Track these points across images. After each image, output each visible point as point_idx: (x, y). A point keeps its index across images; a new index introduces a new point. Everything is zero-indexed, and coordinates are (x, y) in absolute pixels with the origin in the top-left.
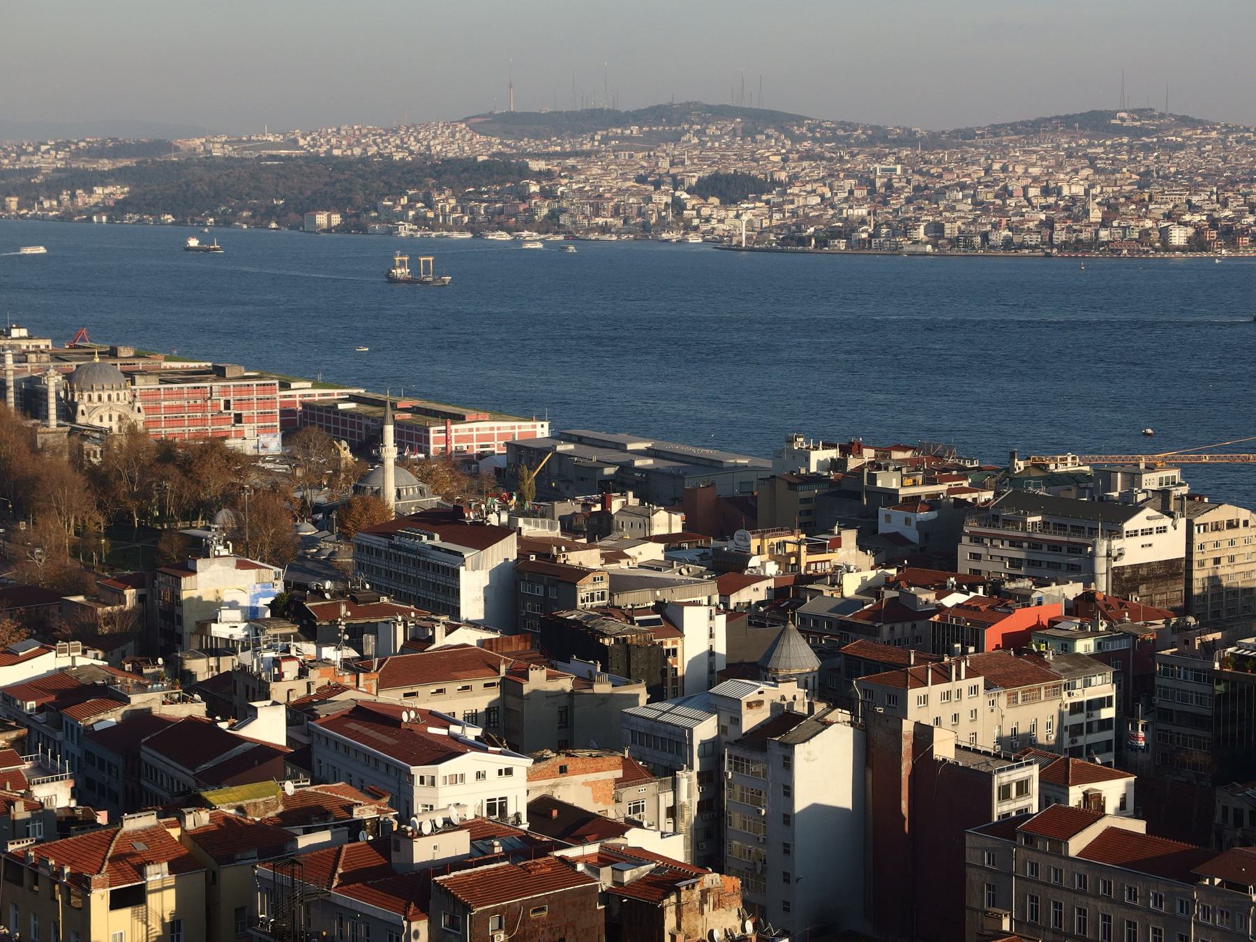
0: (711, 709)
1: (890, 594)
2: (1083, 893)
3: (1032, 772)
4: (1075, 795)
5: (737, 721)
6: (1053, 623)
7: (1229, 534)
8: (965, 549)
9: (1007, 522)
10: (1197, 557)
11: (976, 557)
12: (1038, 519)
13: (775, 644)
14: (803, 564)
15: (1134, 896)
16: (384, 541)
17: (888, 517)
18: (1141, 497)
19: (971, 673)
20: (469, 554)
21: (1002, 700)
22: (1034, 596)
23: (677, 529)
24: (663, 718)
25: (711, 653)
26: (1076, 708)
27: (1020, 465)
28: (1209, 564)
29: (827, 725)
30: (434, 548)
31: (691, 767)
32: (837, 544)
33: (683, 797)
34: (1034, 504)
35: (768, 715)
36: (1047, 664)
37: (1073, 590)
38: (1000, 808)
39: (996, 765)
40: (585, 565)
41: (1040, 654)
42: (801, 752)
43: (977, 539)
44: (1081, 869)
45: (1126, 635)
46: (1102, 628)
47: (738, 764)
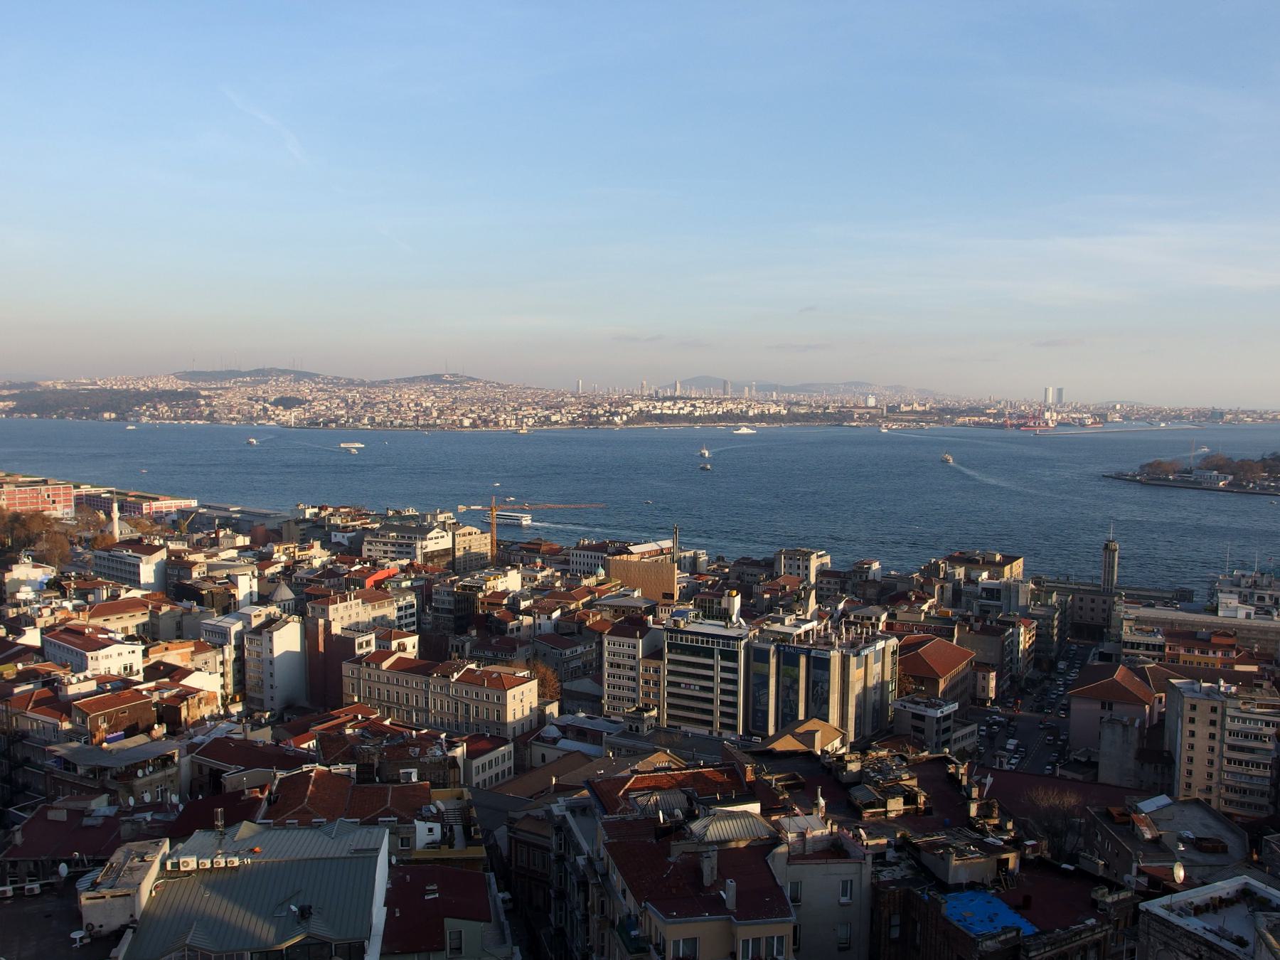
0: (239, 619)
1: (330, 567)
2: (389, 683)
3: (372, 637)
4: (394, 644)
5: (250, 623)
6: (394, 575)
7: (470, 537)
8: (365, 547)
9: (382, 536)
10: (457, 547)
11: (370, 550)
12: (394, 534)
13: (276, 589)
14: (297, 555)
15: (407, 683)
16: (107, 553)
17: (336, 535)
18: (435, 524)
19: (356, 598)
20: (144, 558)
21: (369, 608)
22: (387, 565)
23: (248, 543)
24: (220, 624)
25: (251, 594)
26: (400, 609)
27: (391, 513)
28: (462, 549)
29: (287, 623)
30: (129, 556)
31: (230, 644)
32: (312, 547)
33: (227, 656)
34: (393, 528)
35: (264, 619)
36: (388, 592)
37: (405, 562)
38: (359, 652)
39: (356, 634)
40: (197, 560)
41: (386, 587)
42: (276, 634)
43: (370, 543)
44: (388, 674)
45: (422, 579)
46: (413, 577)
47: (251, 641)
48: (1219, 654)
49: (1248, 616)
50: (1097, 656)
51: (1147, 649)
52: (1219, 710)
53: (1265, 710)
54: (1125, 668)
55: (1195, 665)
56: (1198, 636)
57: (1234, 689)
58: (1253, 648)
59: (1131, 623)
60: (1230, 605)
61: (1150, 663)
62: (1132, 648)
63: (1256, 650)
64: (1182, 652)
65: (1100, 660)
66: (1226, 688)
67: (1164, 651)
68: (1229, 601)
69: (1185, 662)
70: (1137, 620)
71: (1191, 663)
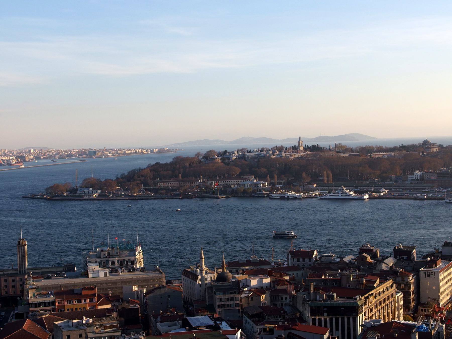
48: (88, 301)
49: (105, 274)
50: (14, 316)
51: (45, 306)
52: (84, 336)
53: (108, 330)
54: (30, 321)
55: (74, 310)
56: (75, 292)
57: (91, 321)
58: (109, 294)
59: (34, 291)
60: (94, 270)
61: (46, 314)
62: (36, 307)
63: (110, 295)
64: (66, 303)
65: (16, 319)
66: (86, 321)
67: (55, 305)
68: (94, 267)
69: (68, 310)
70: (37, 288)
71: (72, 309)
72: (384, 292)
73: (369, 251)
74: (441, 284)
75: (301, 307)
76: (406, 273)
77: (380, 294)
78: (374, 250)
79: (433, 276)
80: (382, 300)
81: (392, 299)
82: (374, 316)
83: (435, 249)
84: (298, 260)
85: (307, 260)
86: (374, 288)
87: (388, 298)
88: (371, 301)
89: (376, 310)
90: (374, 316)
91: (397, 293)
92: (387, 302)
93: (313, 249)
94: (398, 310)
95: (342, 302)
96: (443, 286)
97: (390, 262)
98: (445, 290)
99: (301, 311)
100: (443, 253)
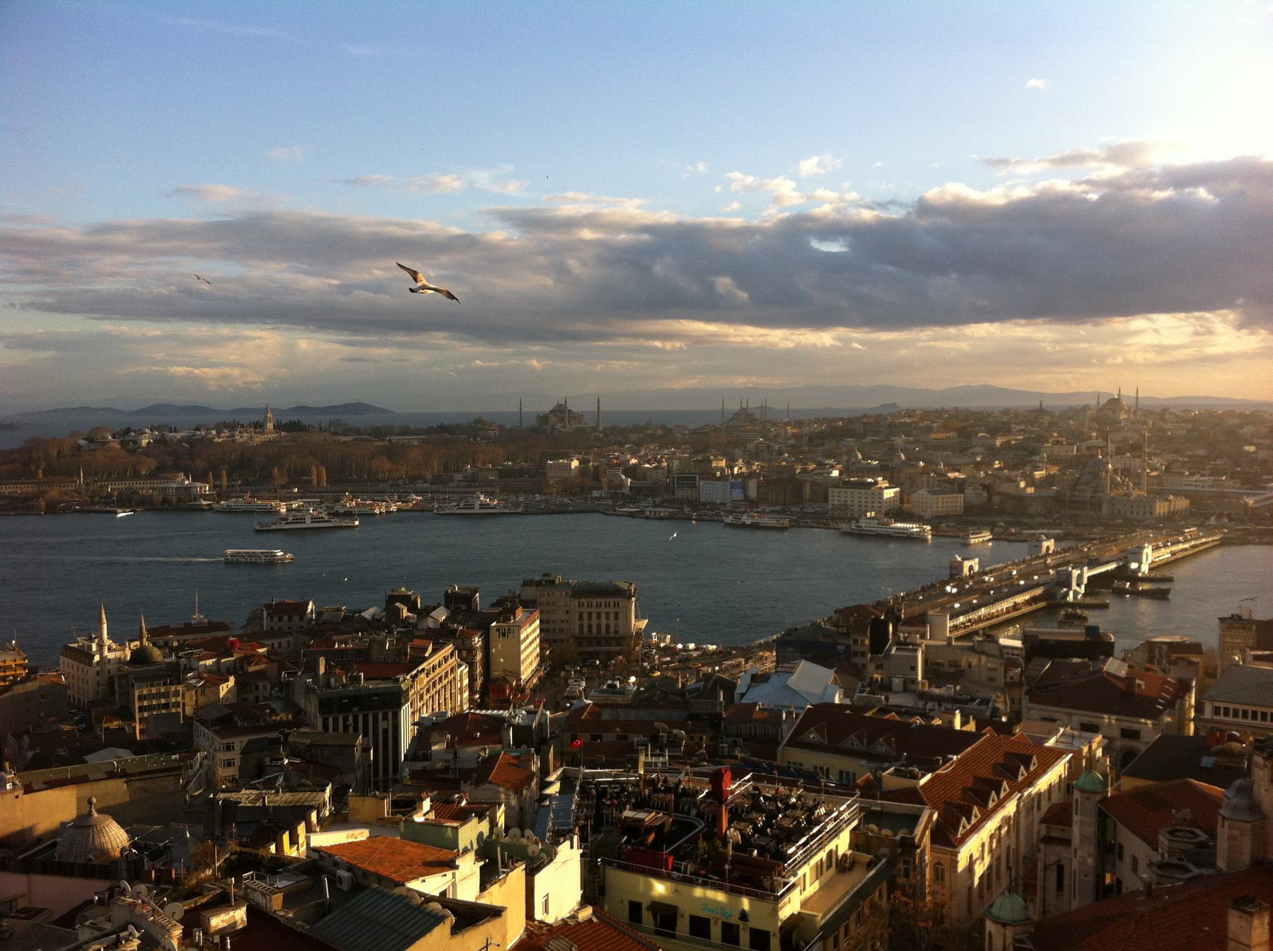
72: (440, 665)
73: (405, 599)
74: (523, 647)
75: (302, 701)
76: (470, 631)
77: (434, 668)
78: (413, 597)
79: (511, 636)
80: (437, 678)
81: (453, 676)
82: (425, 707)
83: (510, 592)
84: (280, 620)
85: (296, 618)
86: (425, 659)
87: (446, 676)
88: (422, 682)
89: (429, 695)
90: (425, 707)
91: (460, 666)
92: (445, 682)
93: (306, 599)
94: (461, 694)
95: (374, 686)
96: (526, 648)
97: (441, 615)
98: (528, 656)
99: (303, 706)
100: (523, 598)
